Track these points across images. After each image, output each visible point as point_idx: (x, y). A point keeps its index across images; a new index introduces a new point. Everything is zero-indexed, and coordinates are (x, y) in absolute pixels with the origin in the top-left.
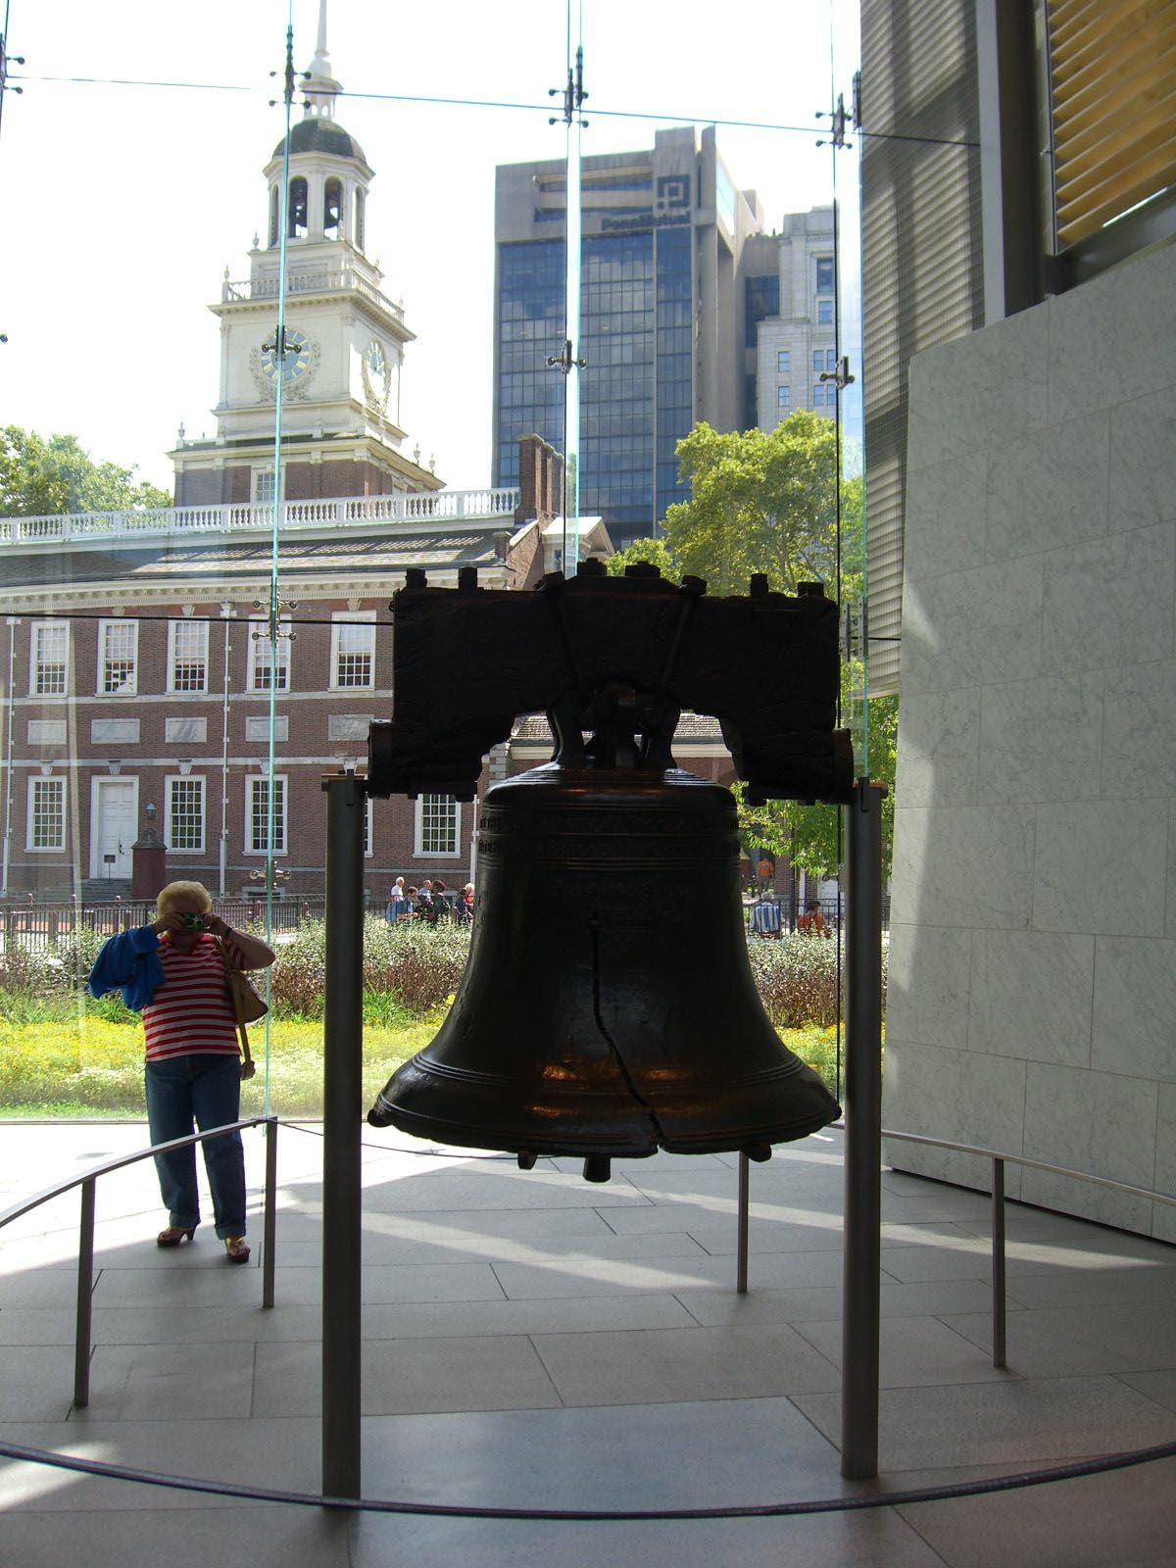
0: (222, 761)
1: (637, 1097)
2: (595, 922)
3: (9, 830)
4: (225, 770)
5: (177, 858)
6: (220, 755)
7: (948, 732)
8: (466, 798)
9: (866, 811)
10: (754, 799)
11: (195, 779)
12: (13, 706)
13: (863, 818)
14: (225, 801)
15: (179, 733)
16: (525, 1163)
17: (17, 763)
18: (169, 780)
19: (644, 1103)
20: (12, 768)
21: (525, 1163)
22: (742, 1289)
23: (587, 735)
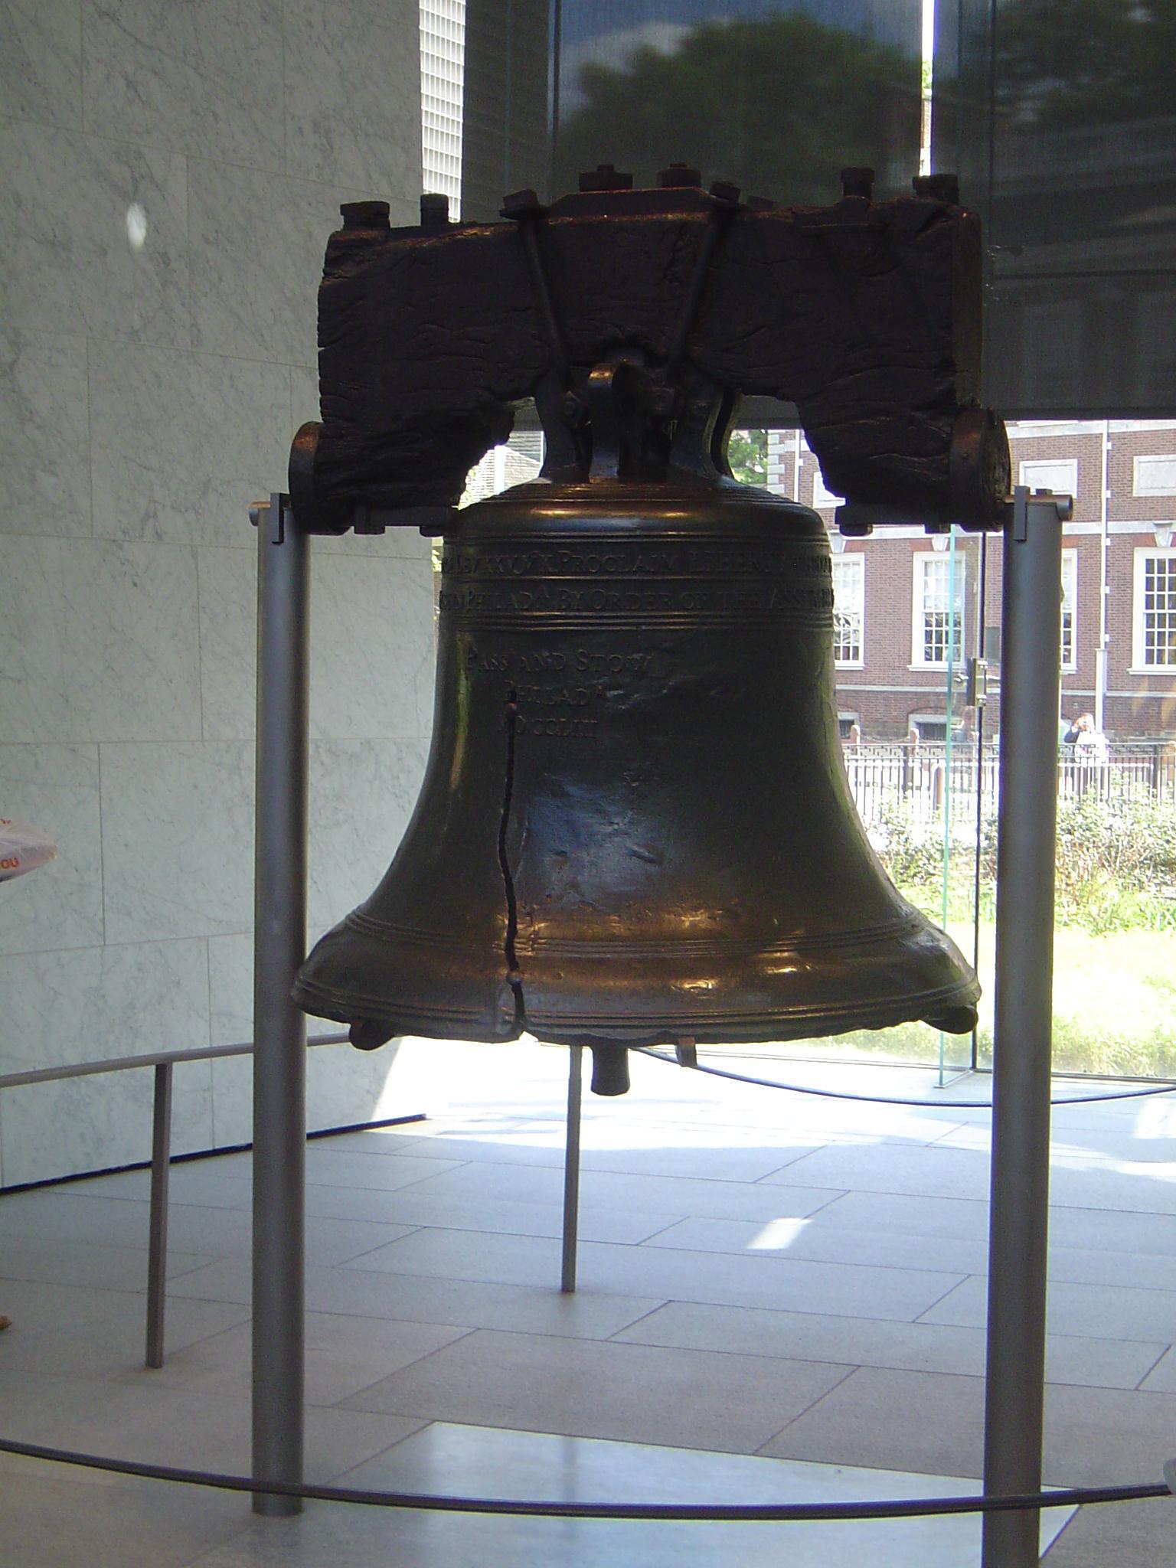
2: (514, 706)
3: (1104, 638)
9: (1023, 541)
10: (853, 523)
12: (1109, 435)
13: (1026, 553)
17: (1116, 527)
20: (1108, 535)
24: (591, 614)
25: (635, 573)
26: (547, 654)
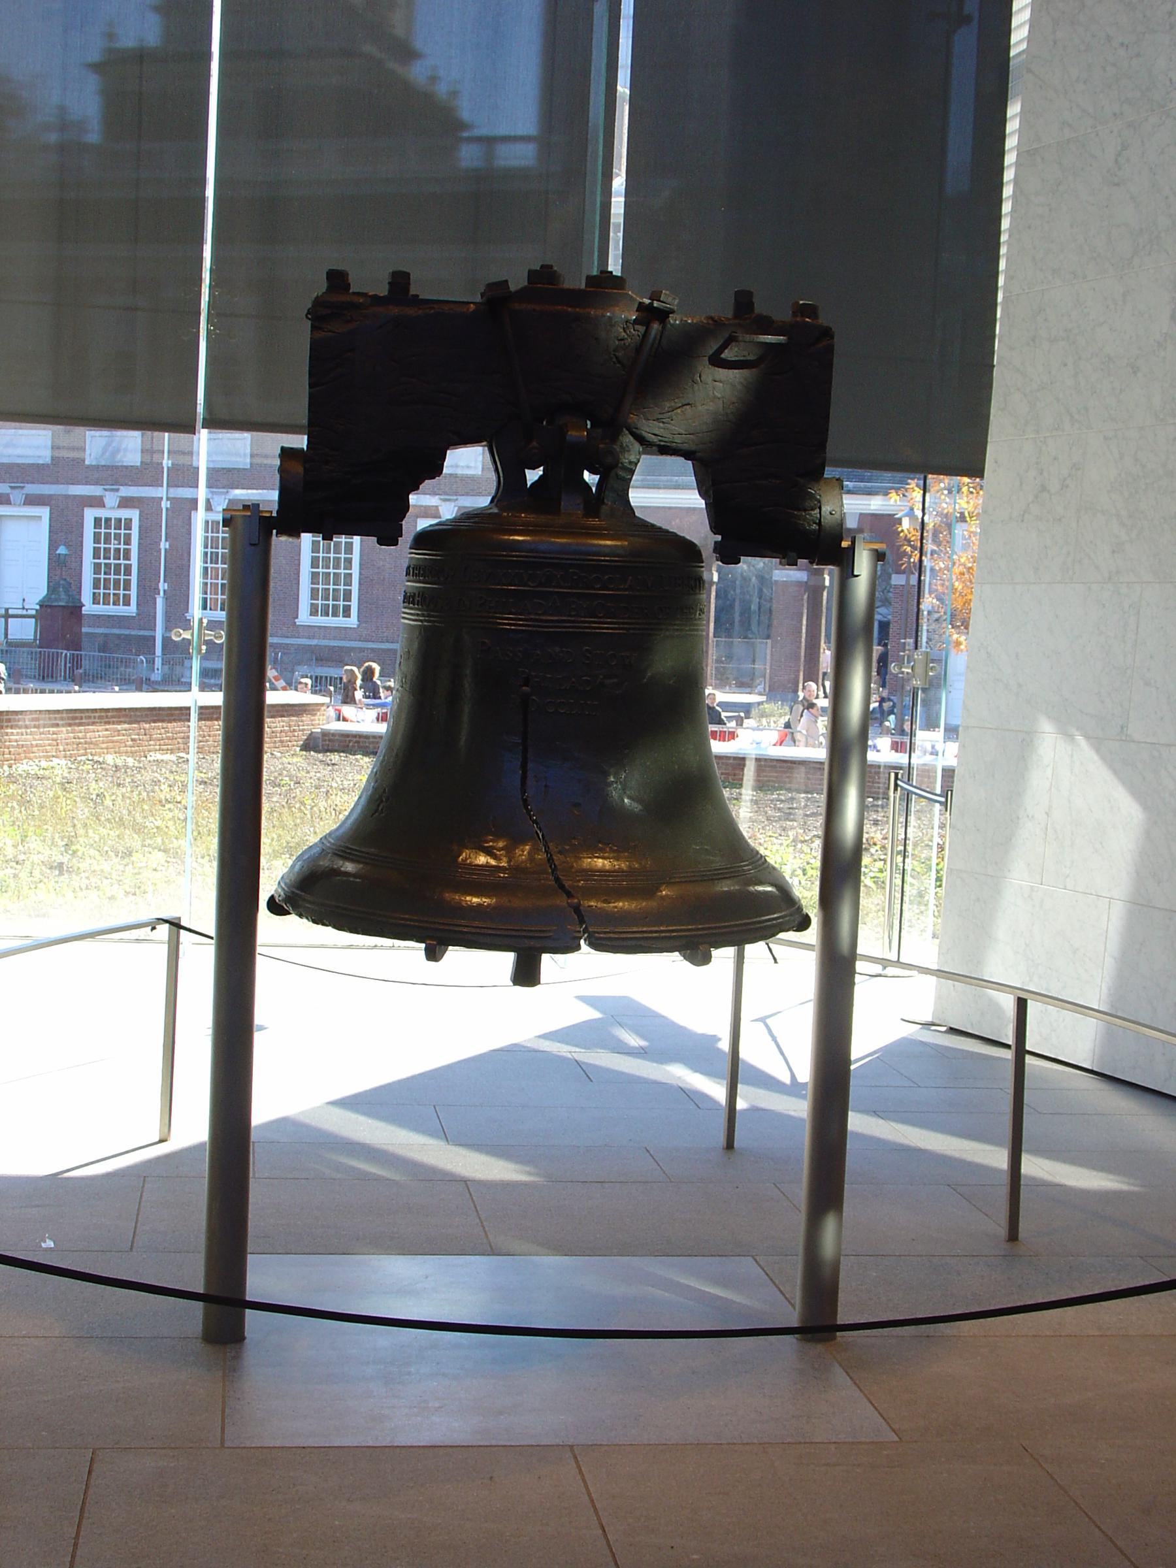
0: (161, 492)
1: (562, 887)
4: (165, 504)
5: (98, 619)
6: (157, 483)
7: (1044, 488)
8: (389, 537)
10: (728, 554)
11: (124, 514)
14: (164, 545)
15: (104, 453)
16: (433, 954)
18: (90, 515)
19: (569, 895)
21: (433, 954)
22: (730, 1145)
23: (533, 476)
24: (596, 620)
25: (626, 590)
26: (557, 649)
